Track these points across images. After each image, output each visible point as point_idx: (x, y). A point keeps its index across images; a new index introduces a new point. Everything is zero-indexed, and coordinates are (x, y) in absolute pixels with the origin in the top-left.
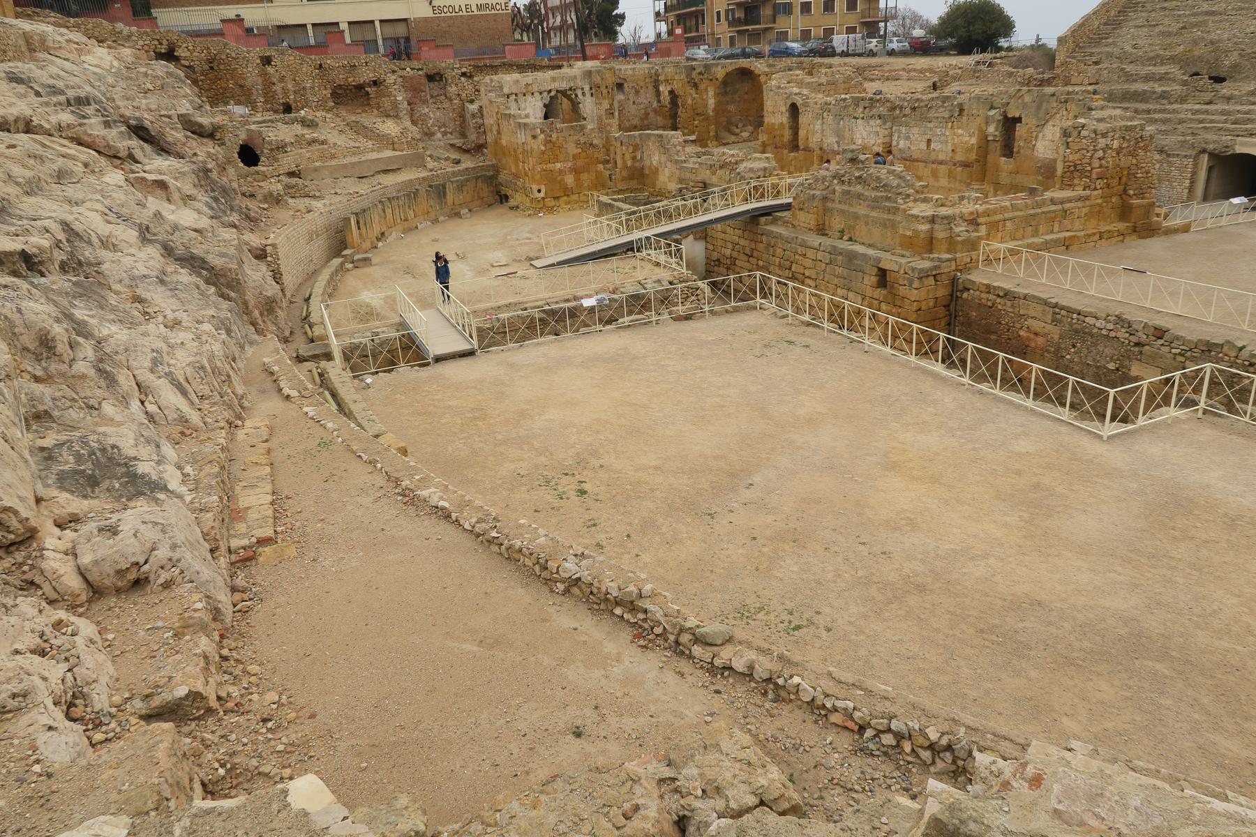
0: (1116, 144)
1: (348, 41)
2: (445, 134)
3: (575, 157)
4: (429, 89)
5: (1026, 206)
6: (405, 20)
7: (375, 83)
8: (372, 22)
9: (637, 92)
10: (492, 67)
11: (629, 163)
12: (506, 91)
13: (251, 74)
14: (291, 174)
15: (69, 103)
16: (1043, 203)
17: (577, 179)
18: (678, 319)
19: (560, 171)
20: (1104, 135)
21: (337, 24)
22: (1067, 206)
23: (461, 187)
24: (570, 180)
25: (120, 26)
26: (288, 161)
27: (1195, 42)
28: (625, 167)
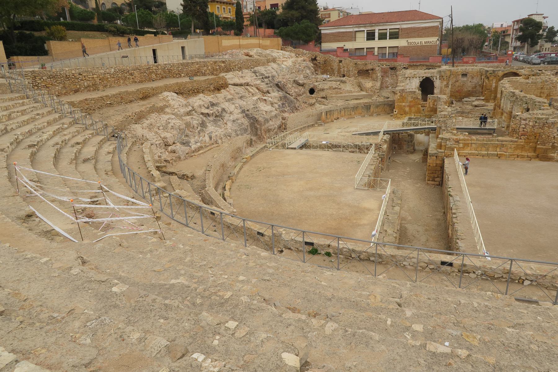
0: (531, 124)
1: (376, 54)
2: (393, 87)
3: (410, 102)
4: (390, 72)
5: (483, 140)
9: (473, 78)
10: (416, 65)
11: (431, 106)
12: (406, 76)
13: (335, 65)
14: (323, 98)
15: (263, 78)
16: (492, 140)
17: (410, 109)
18: (350, 152)
19: (404, 106)
20: (525, 120)
23: (377, 106)
24: (407, 109)
26: (322, 94)
28: (430, 107)
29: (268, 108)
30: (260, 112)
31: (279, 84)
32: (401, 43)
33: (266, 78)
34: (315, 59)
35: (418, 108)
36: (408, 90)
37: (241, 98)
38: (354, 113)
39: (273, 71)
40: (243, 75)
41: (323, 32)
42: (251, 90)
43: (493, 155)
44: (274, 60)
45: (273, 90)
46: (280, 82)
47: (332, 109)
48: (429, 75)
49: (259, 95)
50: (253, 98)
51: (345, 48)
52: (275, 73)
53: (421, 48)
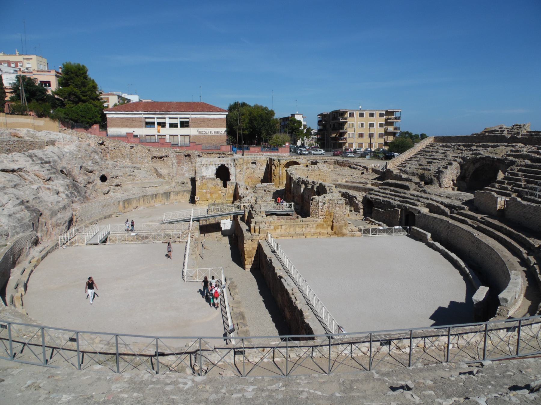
6: (188, 135)
8: (177, 135)
12: (203, 163)
15: (42, 163)
21: (165, 135)
22: (307, 223)
25: (89, 135)
27: (424, 169)
29: (54, 198)
30: (44, 203)
32: (191, 131)
33: (46, 163)
34: (102, 144)
35: (219, 195)
36: (208, 177)
38: (153, 201)
39: (53, 155)
40: (16, 159)
41: (108, 116)
42: (27, 177)
43: (300, 235)
44: (53, 143)
45: (57, 177)
46: (65, 168)
47: (130, 197)
48: (223, 163)
49: (41, 183)
50: (33, 187)
51: (135, 134)
52: (56, 158)
53: (212, 137)
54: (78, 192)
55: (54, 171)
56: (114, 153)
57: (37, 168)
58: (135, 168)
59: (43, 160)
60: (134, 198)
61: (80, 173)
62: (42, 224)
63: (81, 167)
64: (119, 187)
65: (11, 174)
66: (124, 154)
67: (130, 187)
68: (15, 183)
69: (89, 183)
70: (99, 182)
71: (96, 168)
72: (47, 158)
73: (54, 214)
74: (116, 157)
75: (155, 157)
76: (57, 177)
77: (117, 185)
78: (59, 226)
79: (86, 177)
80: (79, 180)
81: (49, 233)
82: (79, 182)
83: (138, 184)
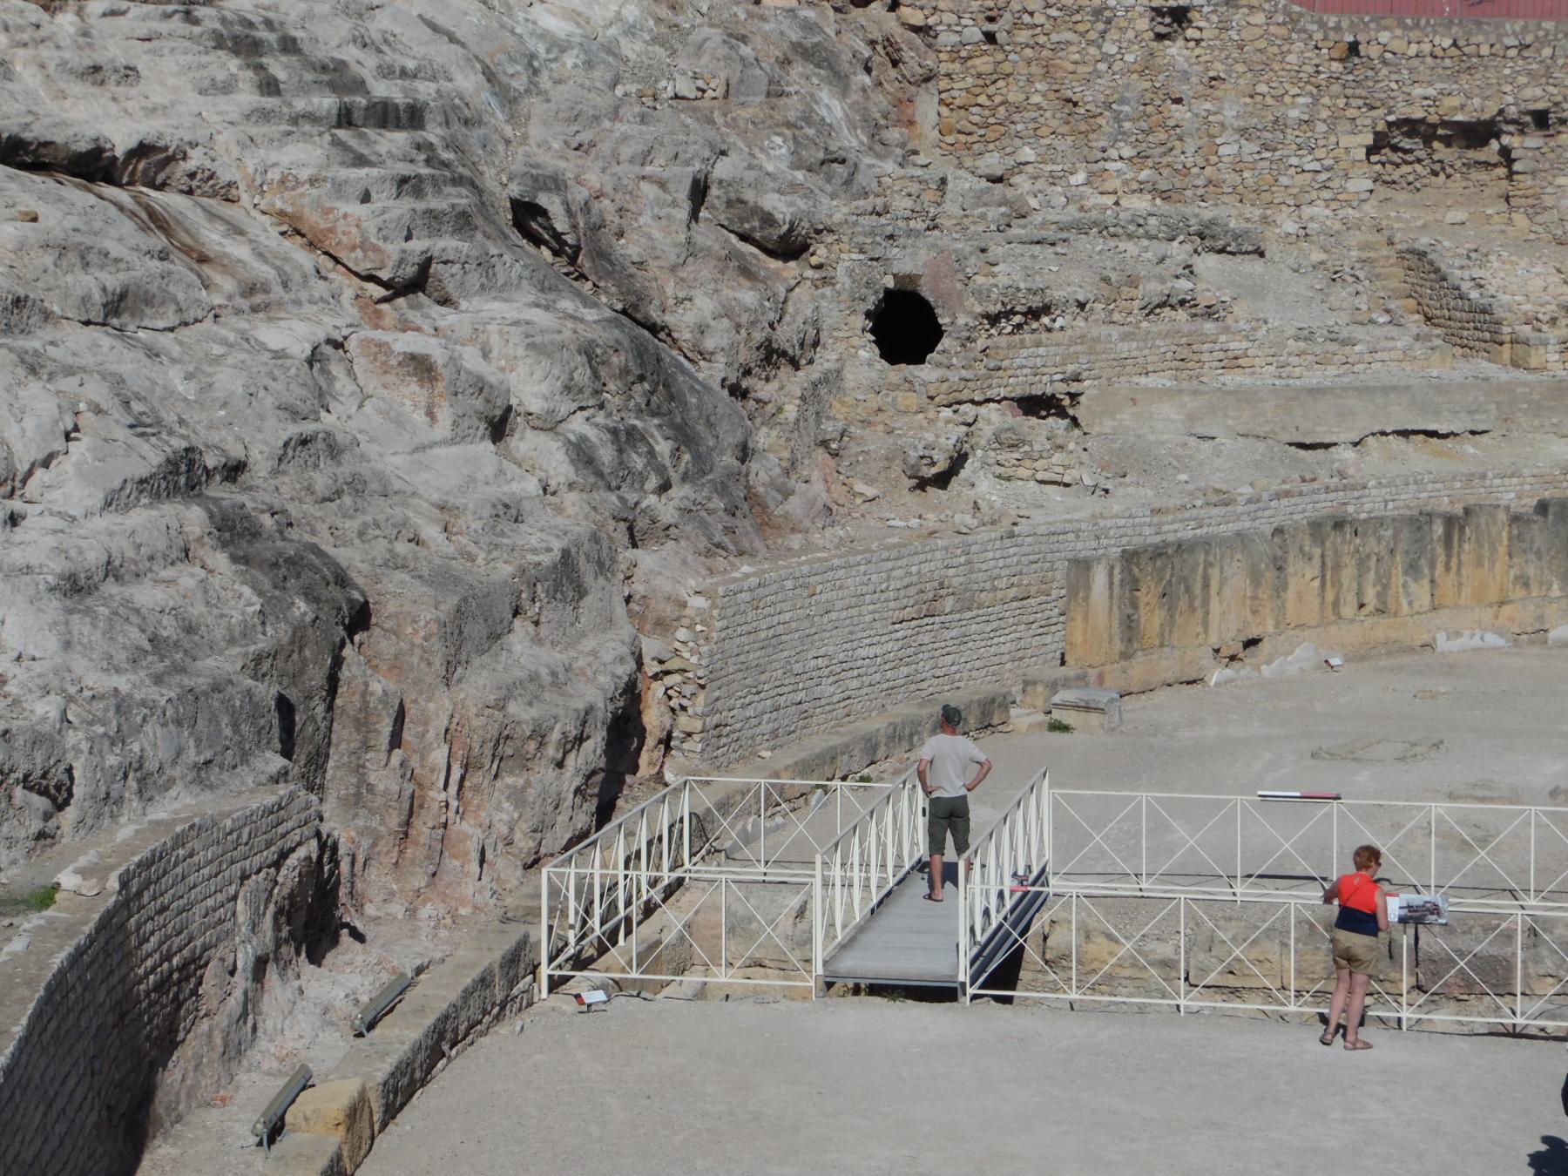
7: (1541, 119)
15: (345, 118)
29: (461, 467)
30: (377, 509)
31: (550, 202)
33: (385, 116)
37: (117, 308)
38: (1421, 592)
39: (443, 53)
40: (114, 52)
42: (213, 237)
45: (485, 264)
46: (556, 184)
47: (1178, 530)
49: (332, 309)
50: (273, 335)
52: (468, 83)
54: (684, 436)
55: (461, 198)
56: (986, 81)
57: (305, 155)
58: (1208, 238)
59: (360, 86)
60: (1226, 543)
61: (691, 250)
62: (363, 723)
63: (699, 192)
64: (1056, 424)
65: (74, 194)
66: (1090, 97)
67: (1164, 423)
68: (114, 281)
69: (771, 355)
70: (855, 355)
71: (834, 209)
72: (386, 72)
73: (475, 625)
74: (998, 126)
75: (1411, 127)
76: (485, 264)
77: (1034, 405)
78: (525, 763)
79: (748, 296)
80: (682, 322)
81: (423, 828)
82: (685, 336)
83: (1246, 397)
